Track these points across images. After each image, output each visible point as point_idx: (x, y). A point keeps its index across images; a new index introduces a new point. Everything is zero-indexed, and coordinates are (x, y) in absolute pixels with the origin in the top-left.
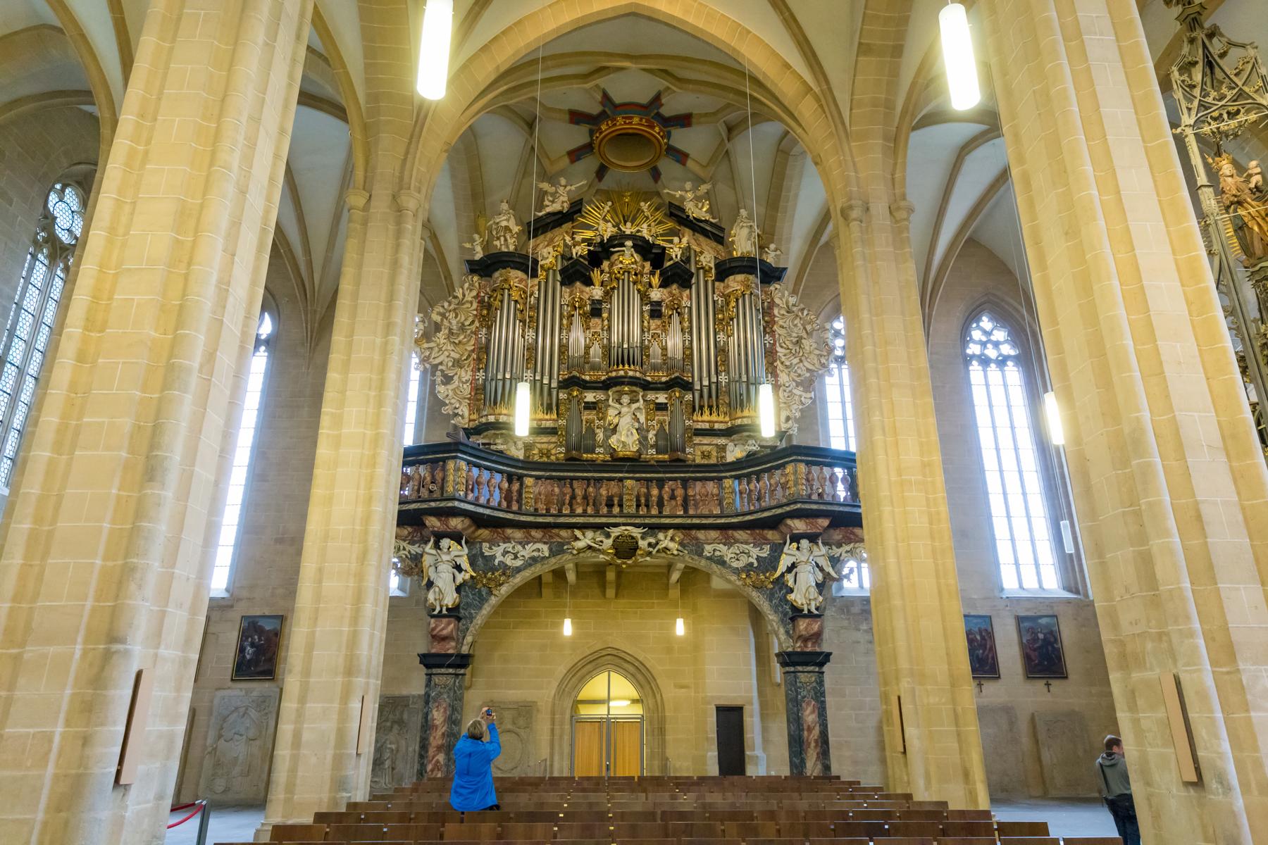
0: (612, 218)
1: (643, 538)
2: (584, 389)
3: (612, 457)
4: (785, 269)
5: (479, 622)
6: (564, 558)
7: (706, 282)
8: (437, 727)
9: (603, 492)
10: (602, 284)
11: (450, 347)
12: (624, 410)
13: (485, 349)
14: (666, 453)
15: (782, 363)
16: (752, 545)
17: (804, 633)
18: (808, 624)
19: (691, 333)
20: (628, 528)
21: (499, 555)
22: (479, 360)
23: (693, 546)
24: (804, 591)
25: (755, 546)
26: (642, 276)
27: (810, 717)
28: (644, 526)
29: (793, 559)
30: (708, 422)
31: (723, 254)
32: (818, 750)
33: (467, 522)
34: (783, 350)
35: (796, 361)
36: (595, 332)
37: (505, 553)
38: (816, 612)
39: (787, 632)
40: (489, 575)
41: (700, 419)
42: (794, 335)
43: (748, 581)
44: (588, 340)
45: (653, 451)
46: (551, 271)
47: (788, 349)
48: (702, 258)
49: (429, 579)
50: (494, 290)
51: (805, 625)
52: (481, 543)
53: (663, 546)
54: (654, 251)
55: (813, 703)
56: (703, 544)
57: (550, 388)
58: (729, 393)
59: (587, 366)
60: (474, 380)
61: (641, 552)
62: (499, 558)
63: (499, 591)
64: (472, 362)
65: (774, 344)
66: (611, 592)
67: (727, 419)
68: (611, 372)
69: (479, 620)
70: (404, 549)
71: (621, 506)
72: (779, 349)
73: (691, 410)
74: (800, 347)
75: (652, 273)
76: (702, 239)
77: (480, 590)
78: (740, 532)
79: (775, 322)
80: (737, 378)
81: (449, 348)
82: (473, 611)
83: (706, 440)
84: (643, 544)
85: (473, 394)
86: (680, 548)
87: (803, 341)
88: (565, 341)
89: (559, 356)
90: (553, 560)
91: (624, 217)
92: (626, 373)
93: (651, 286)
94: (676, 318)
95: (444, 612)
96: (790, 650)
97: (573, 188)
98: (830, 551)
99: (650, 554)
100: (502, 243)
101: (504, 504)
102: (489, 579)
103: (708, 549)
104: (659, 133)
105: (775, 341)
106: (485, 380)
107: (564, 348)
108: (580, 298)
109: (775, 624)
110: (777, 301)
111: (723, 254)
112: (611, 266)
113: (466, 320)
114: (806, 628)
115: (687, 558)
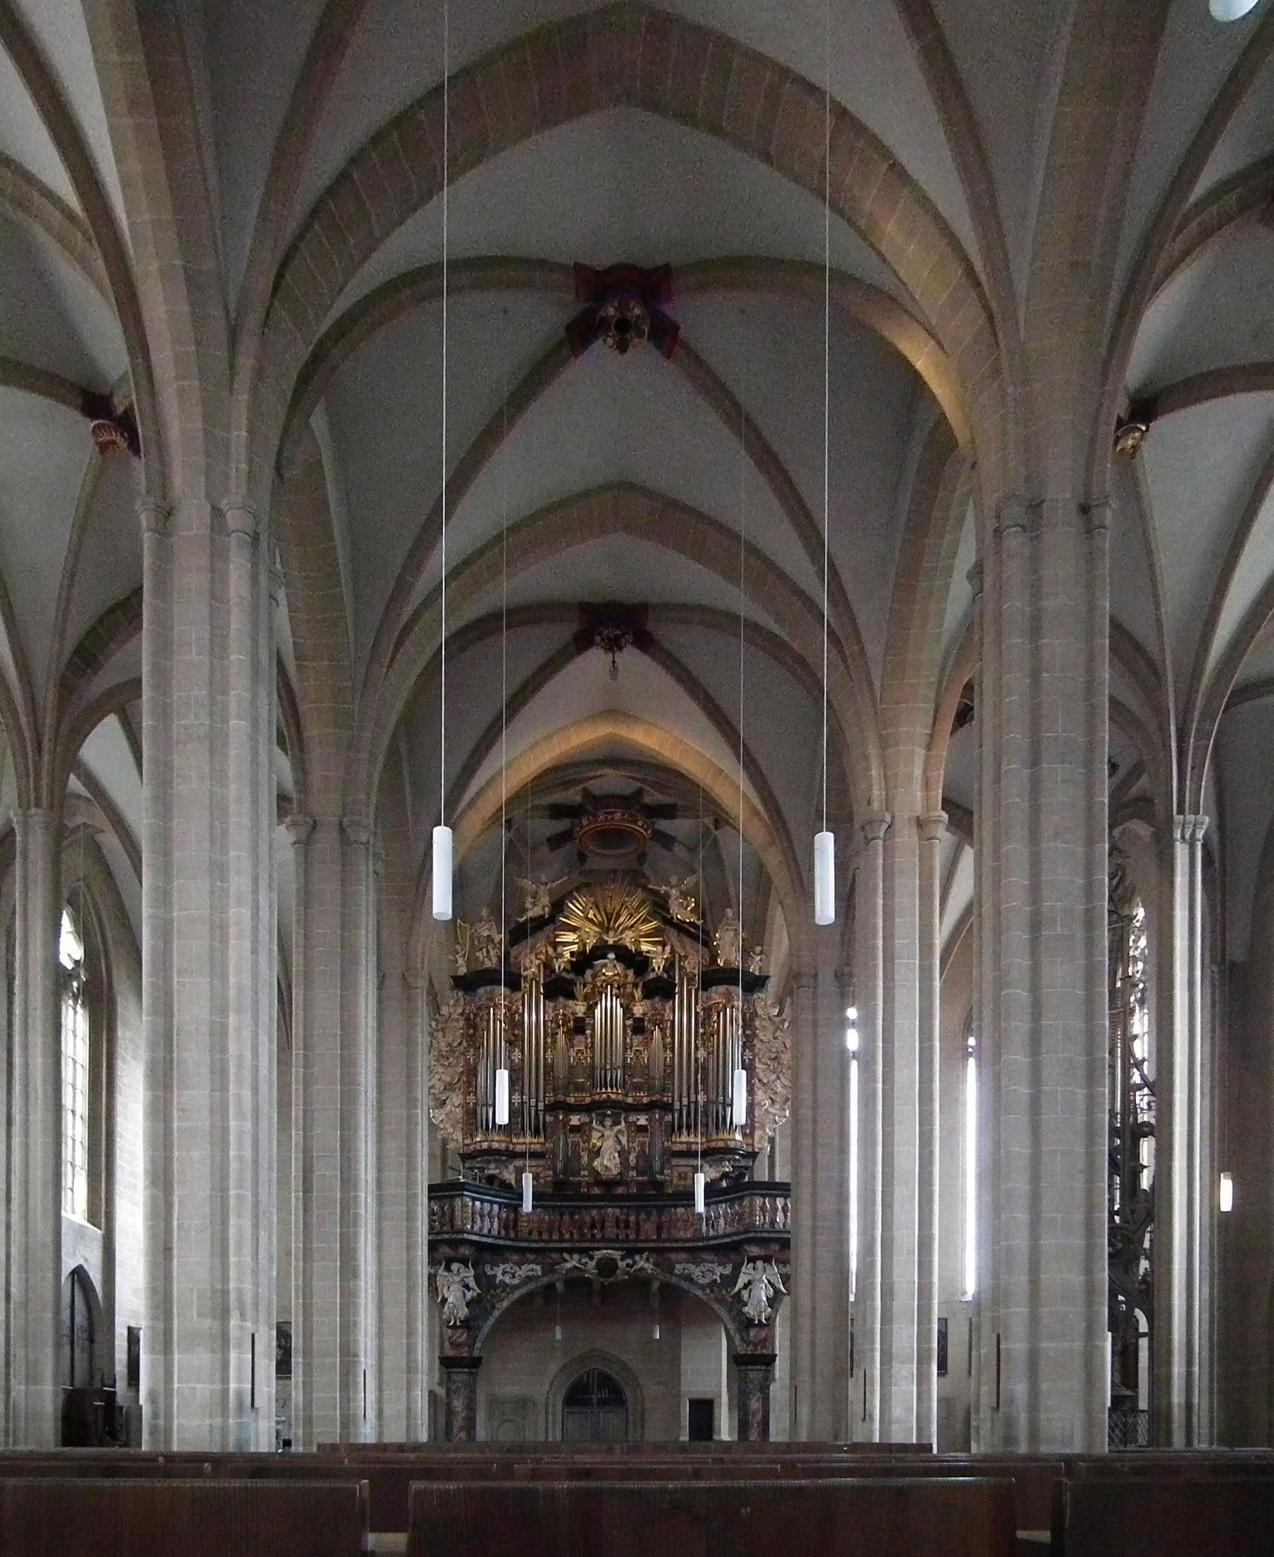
1: (622, 1260)
3: (595, 1179)
4: (767, 977)
8: (457, 1413)
9: (588, 1219)
10: (586, 998)
11: (441, 1070)
12: (607, 1133)
14: (643, 1175)
15: (760, 1081)
19: (673, 1052)
20: (609, 1251)
22: (469, 1084)
25: (719, 1265)
26: (625, 988)
27: (755, 1404)
30: (687, 1143)
32: (760, 1429)
33: (473, 1250)
35: (774, 1077)
37: (504, 1273)
39: (742, 1339)
40: (492, 1292)
41: (678, 1140)
43: (712, 1295)
45: (634, 1173)
47: (767, 1063)
49: (443, 1297)
50: (479, 1008)
54: (637, 959)
57: (537, 1111)
58: (705, 1113)
59: (571, 1087)
62: (501, 1277)
65: (753, 1060)
67: (704, 1140)
69: (486, 1328)
71: (603, 1227)
72: (757, 1065)
73: (669, 1131)
75: (635, 985)
76: (686, 940)
79: (756, 1035)
83: (682, 1162)
84: (621, 1264)
91: (607, 914)
92: (609, 1097)
93: (633, 997)
94: (657, 1033)
95: (458, 1323)
96: (743, 1352)
97: (554, 885)
100: (485, 954)
101: (503, 1232)
102: (492, 1296)
103: (679, 1268)
106: (476, 1104)
107: (549, 1068)
108: (564, 1015)
110: (760, 1012)
112: (594, 976)
113: (454, 1040)
114: (755, 1336)
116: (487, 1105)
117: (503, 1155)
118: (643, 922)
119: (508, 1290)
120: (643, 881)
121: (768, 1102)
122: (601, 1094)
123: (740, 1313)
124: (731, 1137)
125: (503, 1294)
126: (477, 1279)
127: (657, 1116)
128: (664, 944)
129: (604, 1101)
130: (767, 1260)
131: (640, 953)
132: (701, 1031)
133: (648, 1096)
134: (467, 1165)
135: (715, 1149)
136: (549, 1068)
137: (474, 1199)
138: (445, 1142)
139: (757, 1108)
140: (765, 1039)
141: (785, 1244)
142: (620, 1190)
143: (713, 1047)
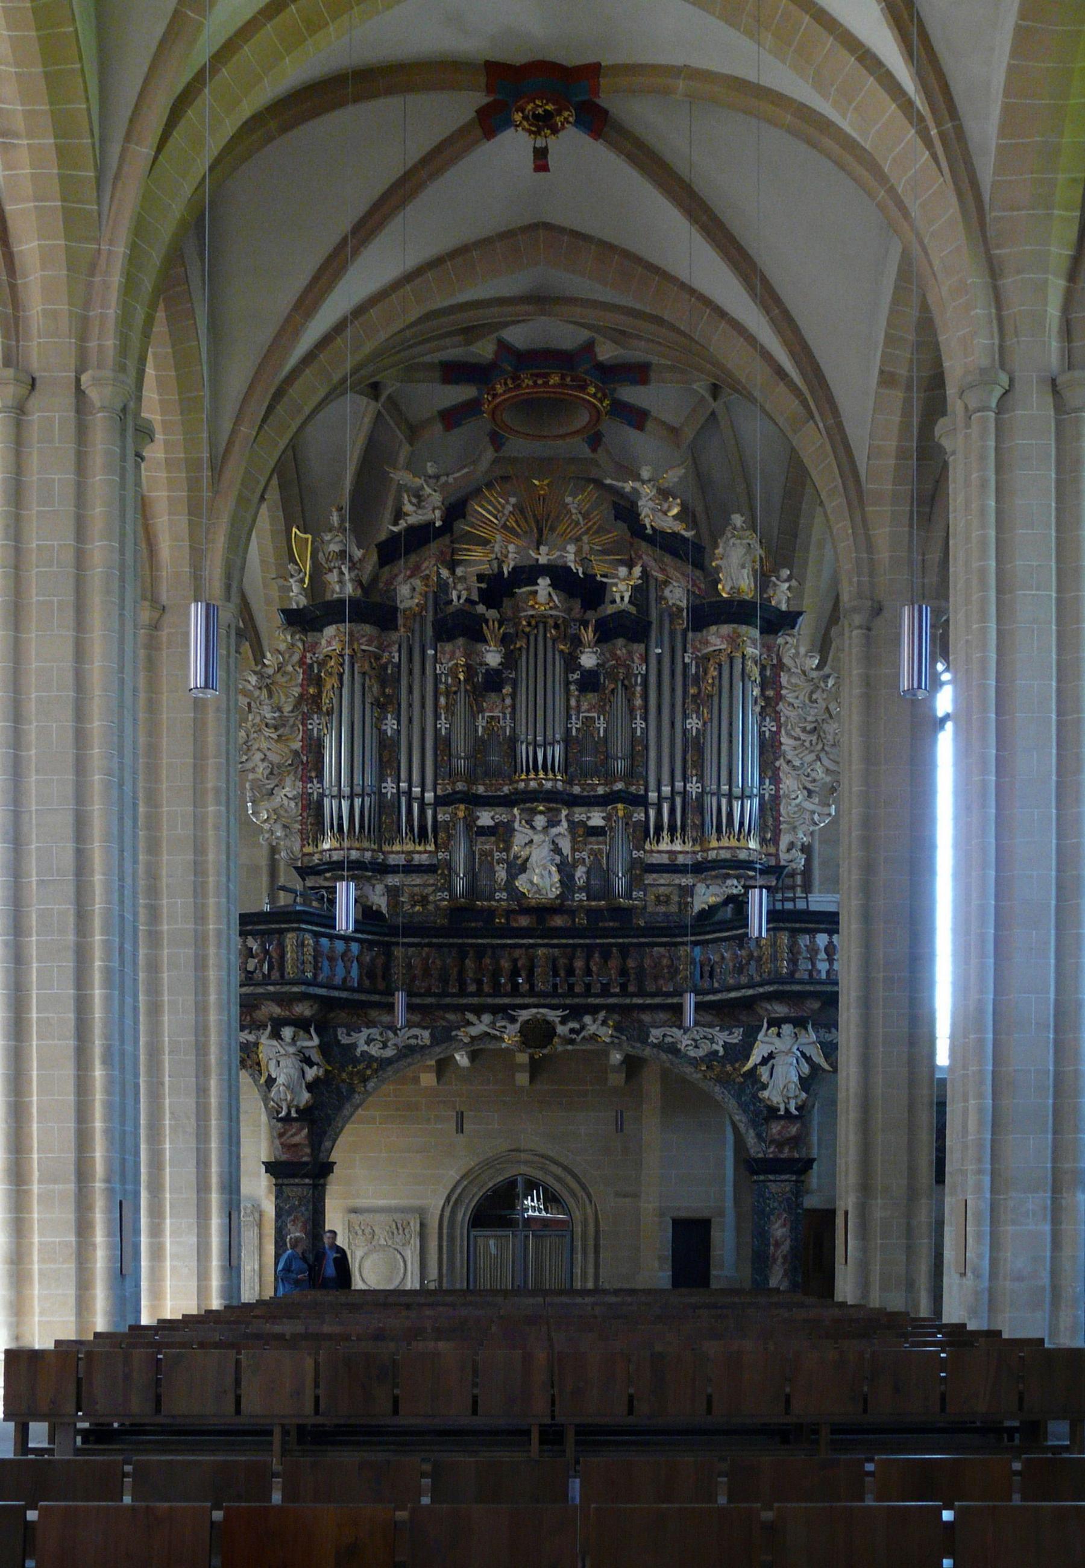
0: (516, 522)
2: (475, 805)
7: (672, 633)
11: (264, 745)
13: (315, 748)
15: (789, 762)
17: (777, 1137)
18: (783, 1127)
19: (645, 719)
21: (362, 1042)
24: (781, 1087)
31: (703, 586)
34: (791, 742)
35: (812, 757)
36: (492, 718)
37: (368, 1042)
38: (796, 1113)
42: (809, 719)
44: (480, 730)
46: (418, 618)
47: (799, 739)
48: (667, 593)
51: (779, 1128)
52: (335, 1029)
53: (591, 1032)
60: (305, 796)
62: (362, 1047)
64: (300, 768)
65: (778, 732)
68: (517, 782)
72: (782, 740)
74: (819, 736)
80: (714, 787)
81: (264, 745)
85: (305, 814)
86: (615, 1034)
87: (825, 726)
88: (443, 732)
89: (436, 755)
90: (438, 1049)
91: (537, 522)
92: (541, 785)
98: (827, 1035)
99: (572, 1042)
102: (351, 1074)
103: (655, 1035)
104: (594, 396)
105: (779, 727)
110: (786, 660)
111: (703, 586)
114: (780, 1133)
116: (340, 796)
117: (367, 870)
118: (597, 532)
119: (375, 1065)
120: (594, 473)
121: (801, 796)
122: (527, 781)
123: (755, 1096)
124: (743, 843)
125: (369, 1072)
126: (323, 1048)
127: (621, 813)
128: (630, 566)
129: (534, 791)
130: (800, 1023)
131: (590, 577)
132: (693, 691)
133: (606, 784)
134: (309, 884)
135: (714, 861)
136: (443, 744)
137: (316, 935)
138: (274, 850)
139: (784, 801)
140: (796, 703)
141: (831, 1000)
142: (558, 921)
143: (711, 712)
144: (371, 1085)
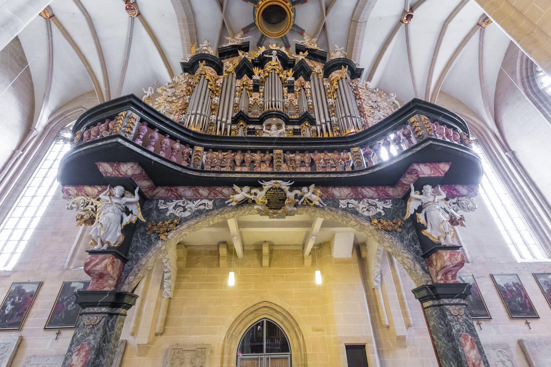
1: (291, 190)
5: (144, 263)
6: (225, 210)
16: (377, 200)
17: (448, 263)
18: (451, 255)
19: (312, 98)
20: (278, 181)
21: (171, 208)
23: (330, 201)
28: (291, 180)
29: (418, 204)
40: (160, 223)
43: (380, 226)
51: (448, 255)
55: (470, 337)
56: (338, 200)
61: (290, 201)
62: (171, 211)
63: (167, 236)
66: (266, 262)
70: (92, 204)
77: (150, 235)
78: (367, 189)
82: (140, 254)
84: (291, 195)
103: (343, 204)
109: (411, 261)
114: (450, 259)
115: (326, 209)
119: (176, 221)
125: (171, 226)
144: (171, 235)
